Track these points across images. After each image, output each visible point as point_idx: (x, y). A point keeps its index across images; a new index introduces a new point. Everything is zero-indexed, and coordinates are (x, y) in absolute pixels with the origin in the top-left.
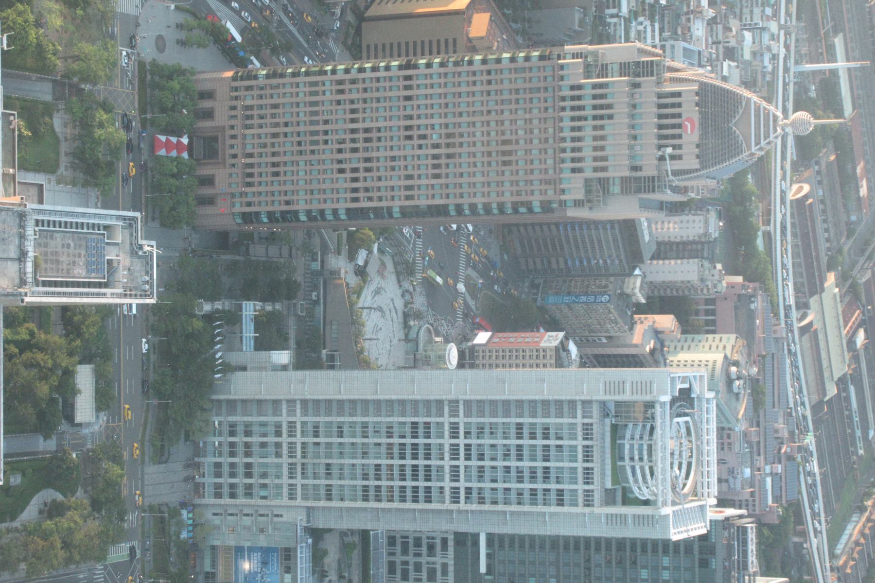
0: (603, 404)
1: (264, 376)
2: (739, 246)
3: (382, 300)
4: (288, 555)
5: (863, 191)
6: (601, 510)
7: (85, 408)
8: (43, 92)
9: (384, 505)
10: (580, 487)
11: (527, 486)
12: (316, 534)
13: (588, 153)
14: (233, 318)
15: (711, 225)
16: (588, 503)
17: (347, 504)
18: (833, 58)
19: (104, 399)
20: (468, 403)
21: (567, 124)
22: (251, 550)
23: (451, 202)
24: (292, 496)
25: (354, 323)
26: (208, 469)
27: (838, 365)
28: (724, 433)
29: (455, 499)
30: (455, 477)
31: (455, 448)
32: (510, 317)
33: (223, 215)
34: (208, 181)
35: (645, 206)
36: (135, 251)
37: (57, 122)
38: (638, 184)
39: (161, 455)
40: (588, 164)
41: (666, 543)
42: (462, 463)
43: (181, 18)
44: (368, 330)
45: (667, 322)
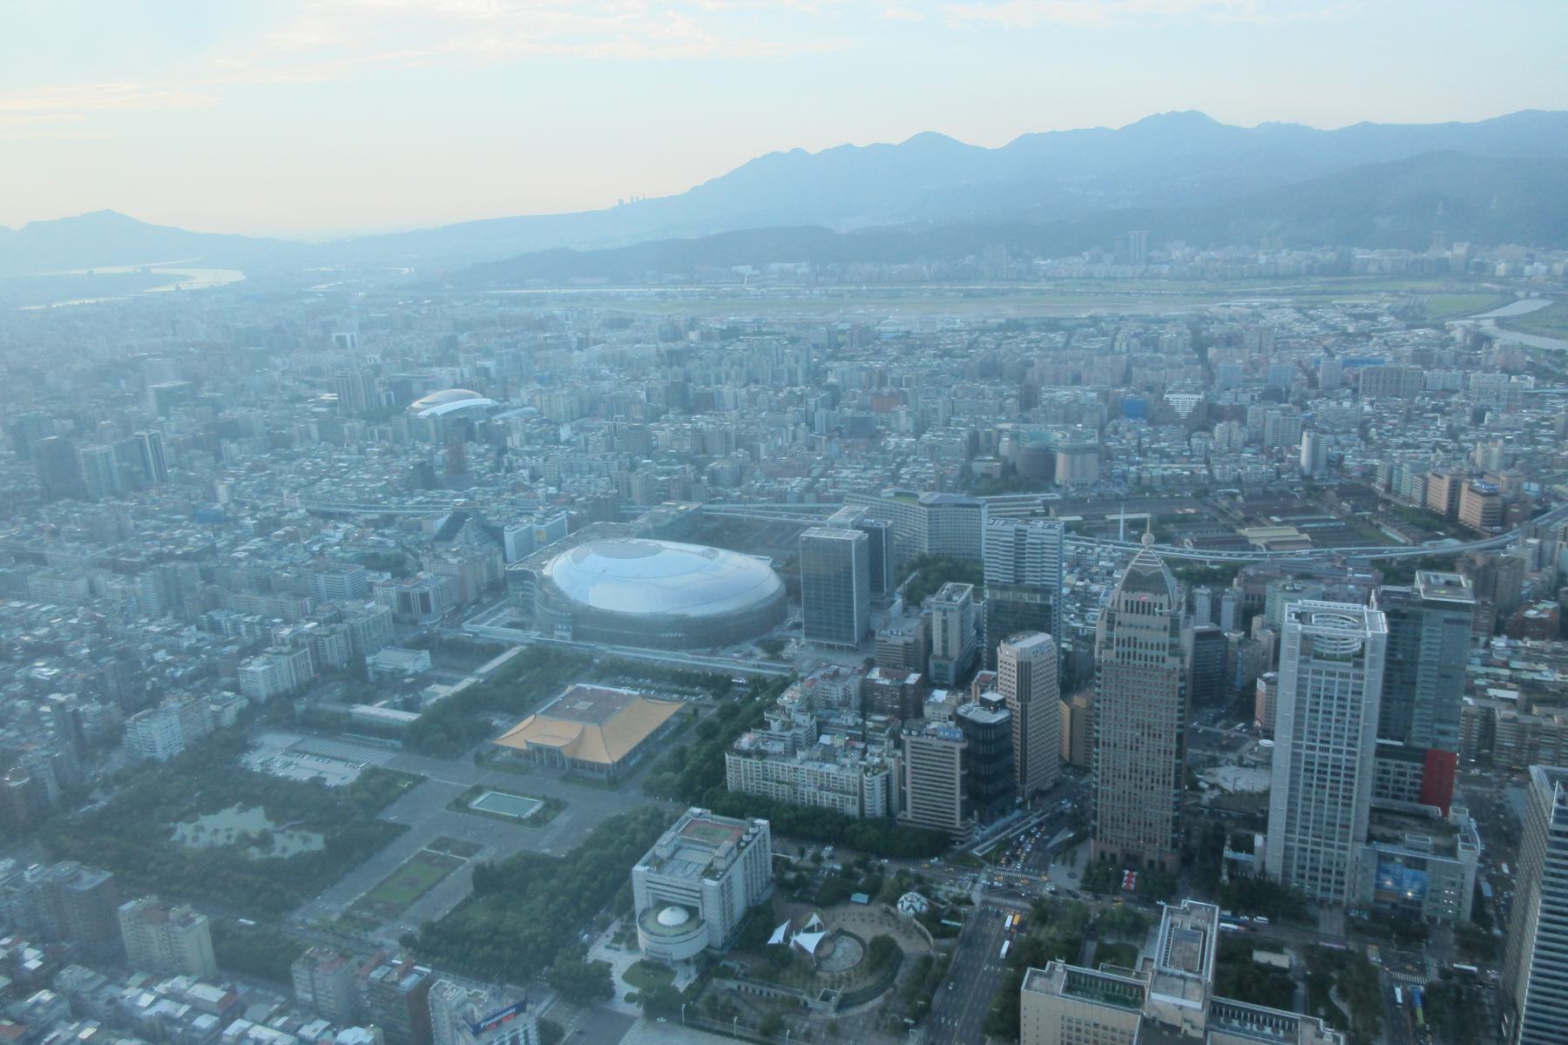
0: (1301, 662)
1: (1270, 850)
2: (1218, 578)
3: (1230, 777)
4: (1383, 857)
5: (1192, 511)
6: (1366, 671)
7: (1281, 961)
8: (1091, 947)
9: (1355, 796)
10: (1351, 681)
11: (1348, 711)
12: (1371, 838)
13: (1154, 653)
14: (1233, 864)
15: (1203, 593)
16: (1362, 678)
17: (1353, 816)
18: (1118, 521)
19: (1276, 948)
20: (1295, 738)
21: (1137, 662)
22: (1378, 878)
23: (1176, 730)
24: (1345, 848)
25: (1241, 795)
26: (1324, 895)
27: (1291, 532)
28: (1325, 597)
29: (1354, 754)
30: (1340, 752)
31: (1322, 749)
32: (1244, 707)
33: (1172, 860)
34: (1151, 863)
35: (1186, 626)
36: (1186, 912)
37: (1109, 942)
38: (1174, 629)
39: (1314, 922)
40: (1160, 653)
41: (1392, 637)
42: (1331, 746)
43: (1059, 862)
44: (1245, 787)
45: (1257, 621)
